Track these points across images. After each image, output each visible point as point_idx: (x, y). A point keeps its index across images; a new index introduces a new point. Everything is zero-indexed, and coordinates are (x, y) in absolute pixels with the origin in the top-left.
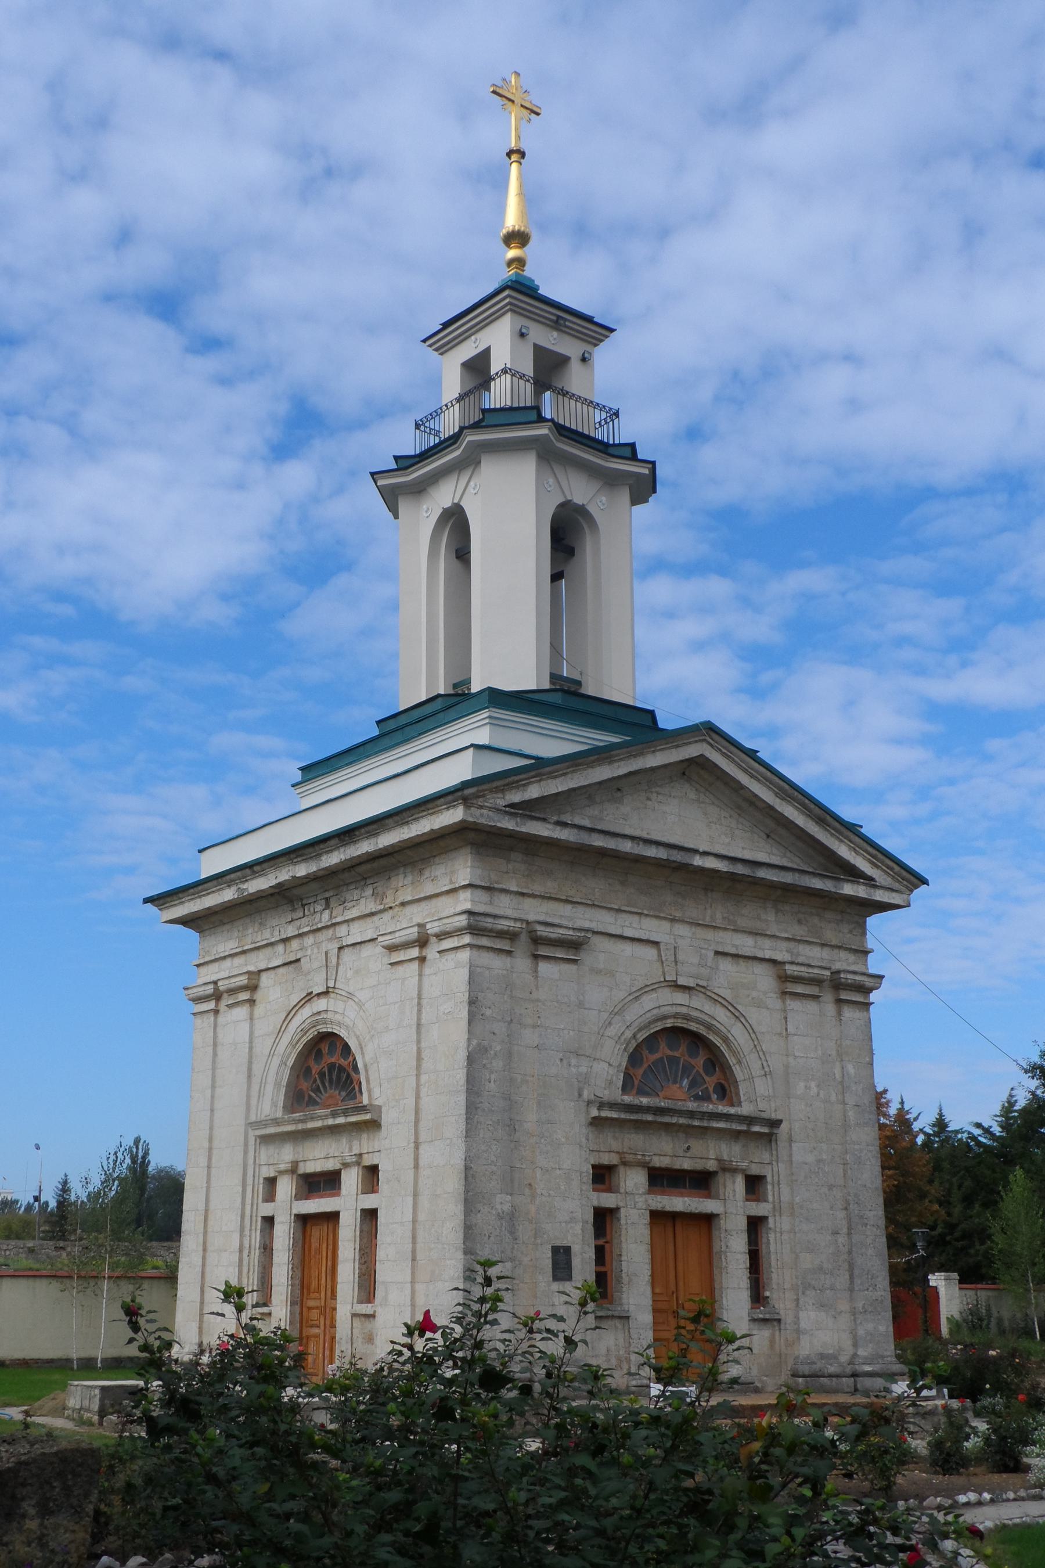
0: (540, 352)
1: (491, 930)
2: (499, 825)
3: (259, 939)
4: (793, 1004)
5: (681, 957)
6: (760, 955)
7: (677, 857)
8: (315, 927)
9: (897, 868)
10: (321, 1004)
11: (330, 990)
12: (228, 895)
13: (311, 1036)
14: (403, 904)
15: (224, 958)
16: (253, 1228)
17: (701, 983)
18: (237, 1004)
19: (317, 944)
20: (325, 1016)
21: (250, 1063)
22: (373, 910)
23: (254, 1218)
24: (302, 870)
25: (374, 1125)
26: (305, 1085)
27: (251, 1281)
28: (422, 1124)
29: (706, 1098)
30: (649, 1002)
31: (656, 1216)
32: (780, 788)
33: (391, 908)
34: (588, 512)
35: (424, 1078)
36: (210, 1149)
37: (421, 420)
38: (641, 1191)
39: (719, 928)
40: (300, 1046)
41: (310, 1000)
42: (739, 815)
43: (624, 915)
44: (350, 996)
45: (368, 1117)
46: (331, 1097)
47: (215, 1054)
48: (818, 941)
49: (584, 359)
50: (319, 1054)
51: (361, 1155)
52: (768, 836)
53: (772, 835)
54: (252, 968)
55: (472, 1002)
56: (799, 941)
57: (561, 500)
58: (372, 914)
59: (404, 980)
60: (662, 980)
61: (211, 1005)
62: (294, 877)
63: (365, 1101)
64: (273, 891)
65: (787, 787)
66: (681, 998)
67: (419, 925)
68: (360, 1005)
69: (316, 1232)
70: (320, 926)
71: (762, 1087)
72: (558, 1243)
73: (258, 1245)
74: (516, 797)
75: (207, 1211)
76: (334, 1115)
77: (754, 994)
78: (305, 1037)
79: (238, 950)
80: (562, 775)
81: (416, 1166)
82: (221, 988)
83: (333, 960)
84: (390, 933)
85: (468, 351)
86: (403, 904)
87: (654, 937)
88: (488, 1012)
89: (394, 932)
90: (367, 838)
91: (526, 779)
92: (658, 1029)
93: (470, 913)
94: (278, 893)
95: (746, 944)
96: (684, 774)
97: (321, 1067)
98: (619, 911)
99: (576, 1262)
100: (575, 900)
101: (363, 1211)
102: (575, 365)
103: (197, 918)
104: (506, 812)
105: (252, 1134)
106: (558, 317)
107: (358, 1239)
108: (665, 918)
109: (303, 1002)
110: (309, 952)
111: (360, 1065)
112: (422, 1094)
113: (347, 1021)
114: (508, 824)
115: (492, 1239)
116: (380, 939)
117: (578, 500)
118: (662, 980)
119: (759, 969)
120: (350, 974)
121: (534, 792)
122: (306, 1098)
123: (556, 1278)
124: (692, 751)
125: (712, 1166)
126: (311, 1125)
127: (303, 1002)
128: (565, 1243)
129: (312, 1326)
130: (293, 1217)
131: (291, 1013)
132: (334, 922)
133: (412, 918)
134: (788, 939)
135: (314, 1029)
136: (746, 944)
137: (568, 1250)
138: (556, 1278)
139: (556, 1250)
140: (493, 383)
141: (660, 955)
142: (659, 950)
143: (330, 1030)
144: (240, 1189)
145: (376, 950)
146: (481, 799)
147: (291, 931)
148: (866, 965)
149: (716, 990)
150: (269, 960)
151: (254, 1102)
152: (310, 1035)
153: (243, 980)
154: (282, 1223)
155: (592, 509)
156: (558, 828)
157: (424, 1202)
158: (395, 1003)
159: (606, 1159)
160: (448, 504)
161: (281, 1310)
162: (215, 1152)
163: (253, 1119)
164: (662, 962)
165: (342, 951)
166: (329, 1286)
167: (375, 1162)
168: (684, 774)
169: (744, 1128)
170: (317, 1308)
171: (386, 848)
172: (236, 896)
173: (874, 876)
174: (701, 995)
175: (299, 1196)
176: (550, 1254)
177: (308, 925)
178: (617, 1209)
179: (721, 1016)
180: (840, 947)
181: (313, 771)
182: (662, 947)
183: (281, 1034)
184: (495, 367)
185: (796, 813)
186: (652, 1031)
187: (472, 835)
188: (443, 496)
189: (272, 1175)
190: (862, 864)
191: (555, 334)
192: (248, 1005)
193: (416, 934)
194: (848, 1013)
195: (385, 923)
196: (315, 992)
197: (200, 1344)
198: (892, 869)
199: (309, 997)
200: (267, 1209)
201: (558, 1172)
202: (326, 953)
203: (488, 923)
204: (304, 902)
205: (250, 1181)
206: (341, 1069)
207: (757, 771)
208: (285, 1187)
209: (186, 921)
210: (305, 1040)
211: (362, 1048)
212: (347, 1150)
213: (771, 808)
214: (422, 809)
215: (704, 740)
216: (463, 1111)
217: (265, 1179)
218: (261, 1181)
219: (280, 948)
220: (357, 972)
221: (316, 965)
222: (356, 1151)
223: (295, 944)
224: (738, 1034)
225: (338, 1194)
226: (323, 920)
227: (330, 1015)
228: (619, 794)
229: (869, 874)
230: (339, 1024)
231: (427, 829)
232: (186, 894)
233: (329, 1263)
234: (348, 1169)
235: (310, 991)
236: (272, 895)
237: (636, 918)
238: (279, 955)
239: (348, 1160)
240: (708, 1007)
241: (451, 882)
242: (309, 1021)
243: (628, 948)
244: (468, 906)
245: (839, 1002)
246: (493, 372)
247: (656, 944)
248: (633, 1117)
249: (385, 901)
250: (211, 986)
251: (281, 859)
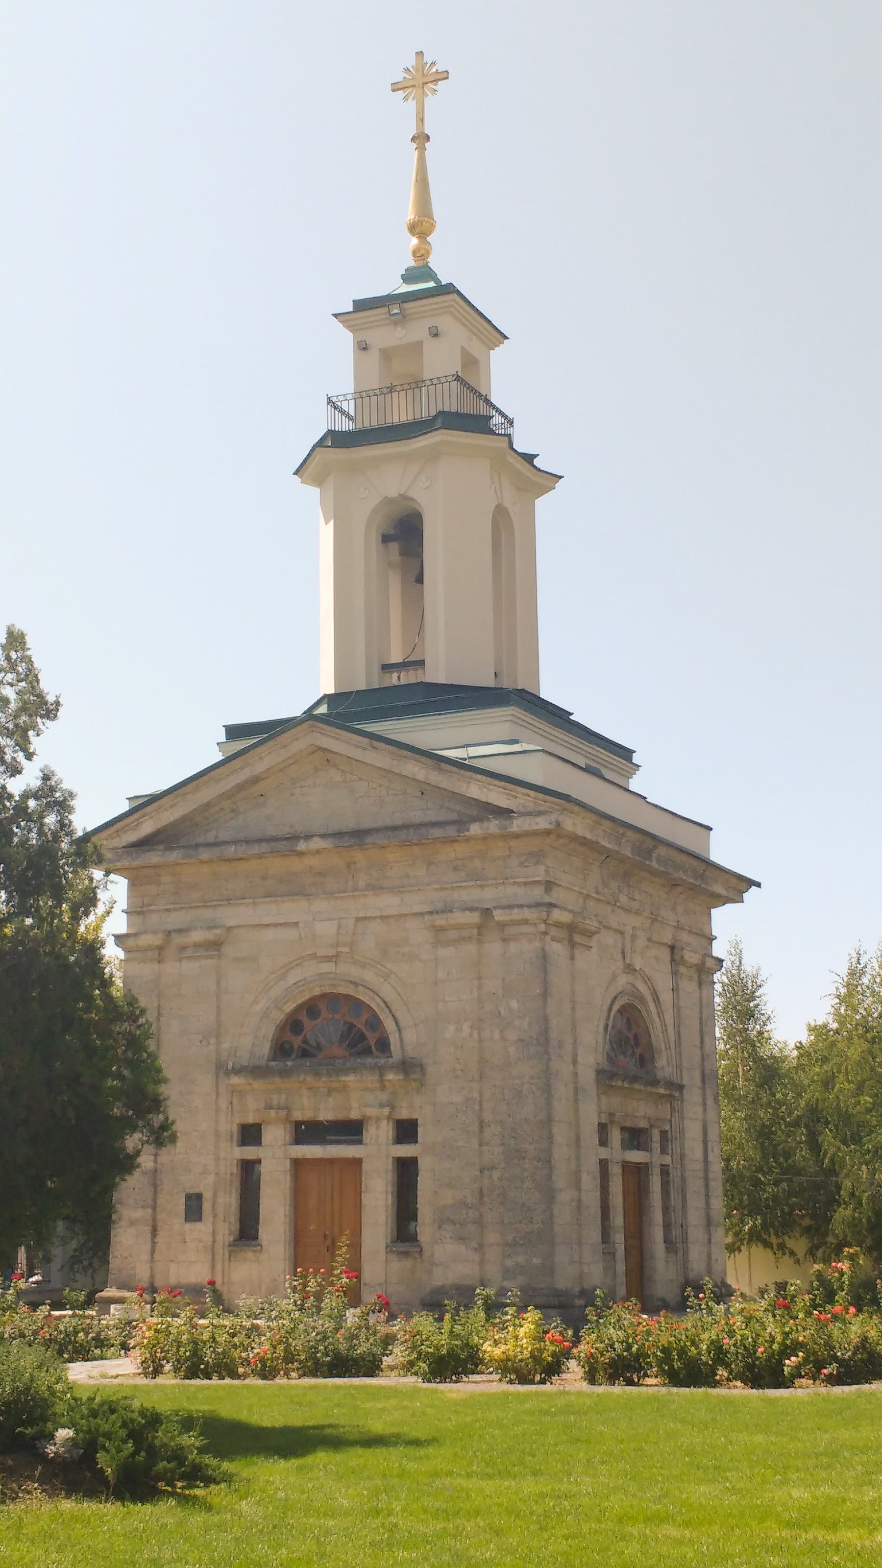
4: (446, 952)
9: (532, 793)
29: (367, 1052)
30: (294, 977)
31: (298, 1164)
38: (281, 1142)
49: (436, 335)
66: (327, 967)
71: (410, 1036)
72: (191, 1191)
74: (133, 837)
77: (406, 949)
80: (171, 807)
99: (207, 1206)
115: (136, 1190)
117: (393, 492)
119: (412, 924)
121: (147, 828)
123: (188, 1219)
125: (354, 1115)
128: (197, 1191)
137: (199, 1197)
138: (188, 1219)
139: (189, 1197)
155: (411, 494)
159: (251, 1119)
176: (183, 1200)
178: (259, 1161)
179: (369, 976)
185: (416, 769)
186: (300, 1002)
190: (497, 796)
194: (513, 947)
201: (195, 1134)
215: (313, 731)
224: (387, 991)
228: (262, 799)
240: (355, 972)
243: (270, 934)
245: (505, 940)
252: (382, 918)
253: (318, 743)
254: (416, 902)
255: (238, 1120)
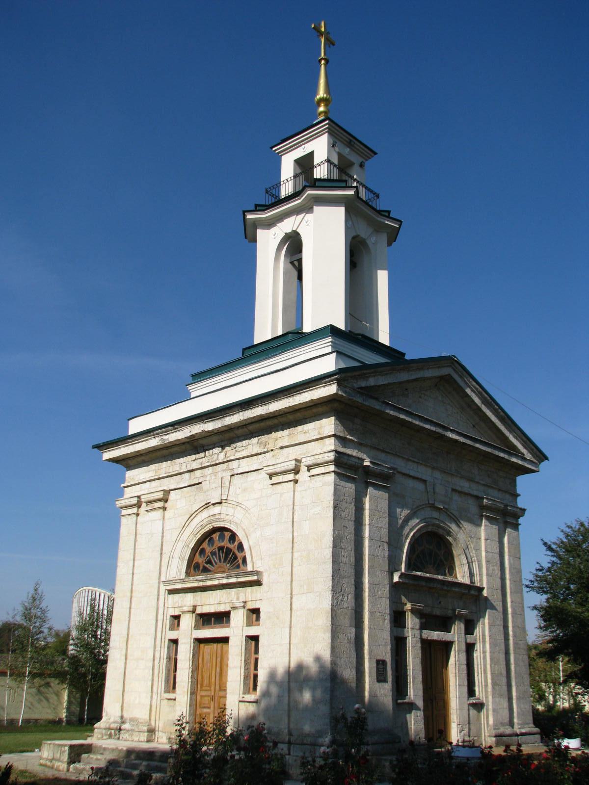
0: (340, 156)
1: (346, 464)
2: (354, 399)
3: (171, 470)
5: (437, 490)
6: (472, 492)
7: (440, 431)
8: (214, 463)
9: (535, 450)
10: (217, 509)
11: (223, 501)
12: (153, 442)
13: (207, 530)
14: (282, 448)
15: (145, 482)
16: (163, 646)
17: (446, 507)
18: (154, 509)
19: (215, 473)
20: (219, 517)
21: (162, 545)
22: (259, 452)
23: (163, 640)
24: (210, 426)
25: (258, 583)
26: (199, 559)
27: (160, 679)
28: (294, 583)
32: (485, 398)
33: (272, 450)
34: (366, 243)
35: (296, 555)
36: (131, 597)
37: (270, 188)
39: (454, 475)
40: (199, 536)
41: (207, 507)
42: (461, 413)
43: (410, 463)
44: (239, 504)
45: (255, 578)
46: (220, 567)
47: (136, 540)
48: (497, 487)
50: (211, 542)
51: (245, 602)
52: (474, 426)
53: (476, 426)
54: (166, 488)
55: (335, 507)
56: (489, 486)
57: (355, 234)
58: (258, 454)
59: (282, 494)
60: (427, 502)
61: (135, 510)
62: (204, 432)
63: (250, 568)
64: (188, 440)
65: (489, 398)
67: (296, 460)
68: (246, 510)
69: (207, 648)
70: (218, 462)
73: (165, 657)
74: (363, 384)
75: (128, 635)
76: (228, 577)
78: (203, 530)
79: (156, 477)
81: (291, 609)
82: (143, 500)
83: (227, 484)
84: (274, 465)
85: (299, 153)
86: (282, 448)
87: (424, 478)
88: (343, 514)
89: (276, 464)
90: (261, 406)
91: (369, 373)
92: (424, 531)
93: (336, 452)
94: (188, 442)
95: (465, 485)
96: (436, 385)
97: (213, 548)
98: (408, 460)
100: (387, 451)
101: (247, 637)
102: (356, 167)
103: (127, 458)
104: (359, 392)
105: (163, 588)
106: (351, 140)
107: (243, 654)
108: (430, 467)
109: (202, 508)
110: (208, 478)
111: (246, 546)
112: (295, 565)
113: (236, 520)
114: (359, 399)
116: (265, 469)
118: (427, 502)
120: (238, 491)
121: (372, 382)
122: (201, 568)
124: (445, 371)
126: (209, 583)
127: (202, 508)
129: (204, 707)
130: (192, 640)
131: (192, 516)
132: (229, 459)
133: (288, 457)
134: (484, 485)
135: (210, 525)
136: (465, 485)
138: (379, 681)
139: (378, 662)
140: (315, 169)
141: (426, 488)
142: (426, 485)
143: (223, 526)
144: (154, 622)
145: (263, 475)
146: (346, 382)
147: (195, 465)
148: (516, 503)
149: (452, 511)
150: (178, 483)
151: (164, 569)
152: (207, 529)
153: (160, 495)
154: (185, 643)
156: (384, 405)
157: (297, 632)
158: (277, 508)
160: (289, 230)
161: (184, 697)
162: (133, 599)
163: (163, 579)
164: (427, 492)
165: (233, 477)
166: (217, 683)
167: (257, 607)
168: (436, 385)
169: (467, 591)
170: (208, 696)
171: (274, 412)
172: (159, 444)
173: (524, 453)
174: (444, 513)
175: (197, 627)
176: (375, 665)
177: (209, 462)
180: (506, 492)
181: (199, 376)
182: (428, 482)
183: (184, 528)
184: (316, 161)
187: (336, 405)
188: (287, 226)
189: (177, 613)
191: (348, 149)
192: (161, 510)
193: (294, 465)
195: (267, 459)
196: (212, 503)
197: (122, 717)
198: (532, 450)
199: (207, 505)
200: (173, 635)
202: (222, 478)
203: (345, 459)
204: (206, 448)
205: (160, 617)
206: (229, 550)
207: (475, 387)
208: (187, 621)
209: (116, 460)
210: (203, 532)
211: (247, 537)
212: (235, 599)
213: (479, 409)
214: (306, 386)
215: (450, 366)
216: (330, 575)
217: (171, 616)
218: (169, 617)
219: (187, 475)
220: (245, 490)
221: (213, 486)
222: (242, 599)
223: (198, 473)
225: (229, 627)
226: (220, 458)
227: (222, 516)
229: (522, 451)
230: (230, 522)
231: (308, 399)
232: (124, 442)
233: (218, 669)
234: (236, 611)
235: (208, 502)
236: (184, 443)
237: (415, 465)
238: (186, 479)
239: (237, 605)
241: (319, 433)
242: (206, 520)
244: (333, 448)
246: (316, 163)
247: (424, 481)
248: (416, 583)
249: (267, 446)
250: (136, 499)
251: (196, 420)
252: (460, 492)
253: (452, 375)
254: (475, 490)
255: (394, 609)
